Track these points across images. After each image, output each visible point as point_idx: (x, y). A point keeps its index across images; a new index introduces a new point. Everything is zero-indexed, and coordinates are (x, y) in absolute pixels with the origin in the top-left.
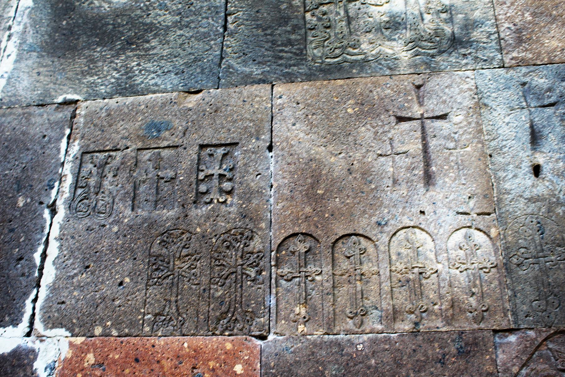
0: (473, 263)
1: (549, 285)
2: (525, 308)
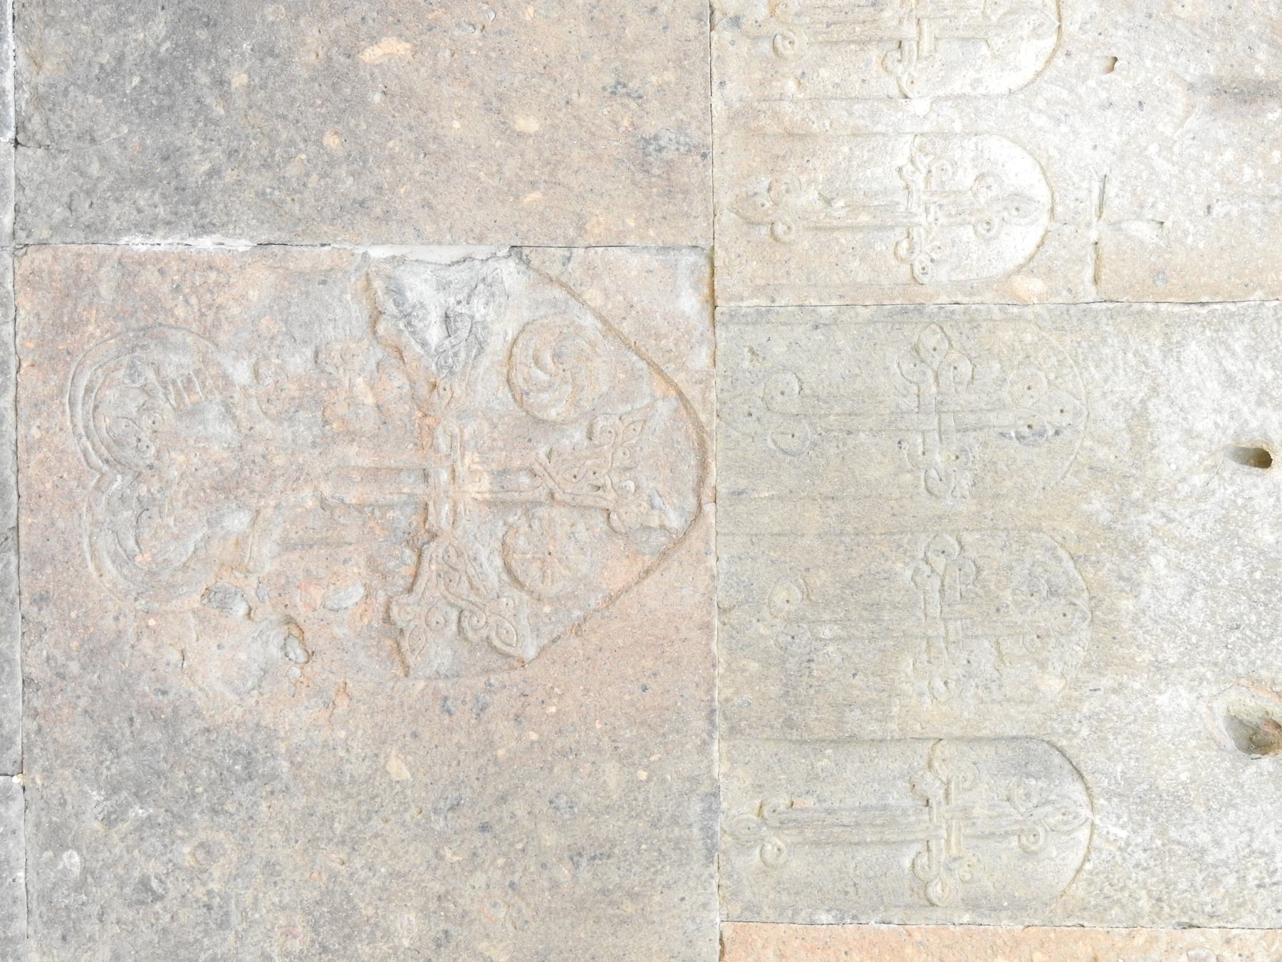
0: (927, 210)
1: (849, 433)
2: (776, 350)
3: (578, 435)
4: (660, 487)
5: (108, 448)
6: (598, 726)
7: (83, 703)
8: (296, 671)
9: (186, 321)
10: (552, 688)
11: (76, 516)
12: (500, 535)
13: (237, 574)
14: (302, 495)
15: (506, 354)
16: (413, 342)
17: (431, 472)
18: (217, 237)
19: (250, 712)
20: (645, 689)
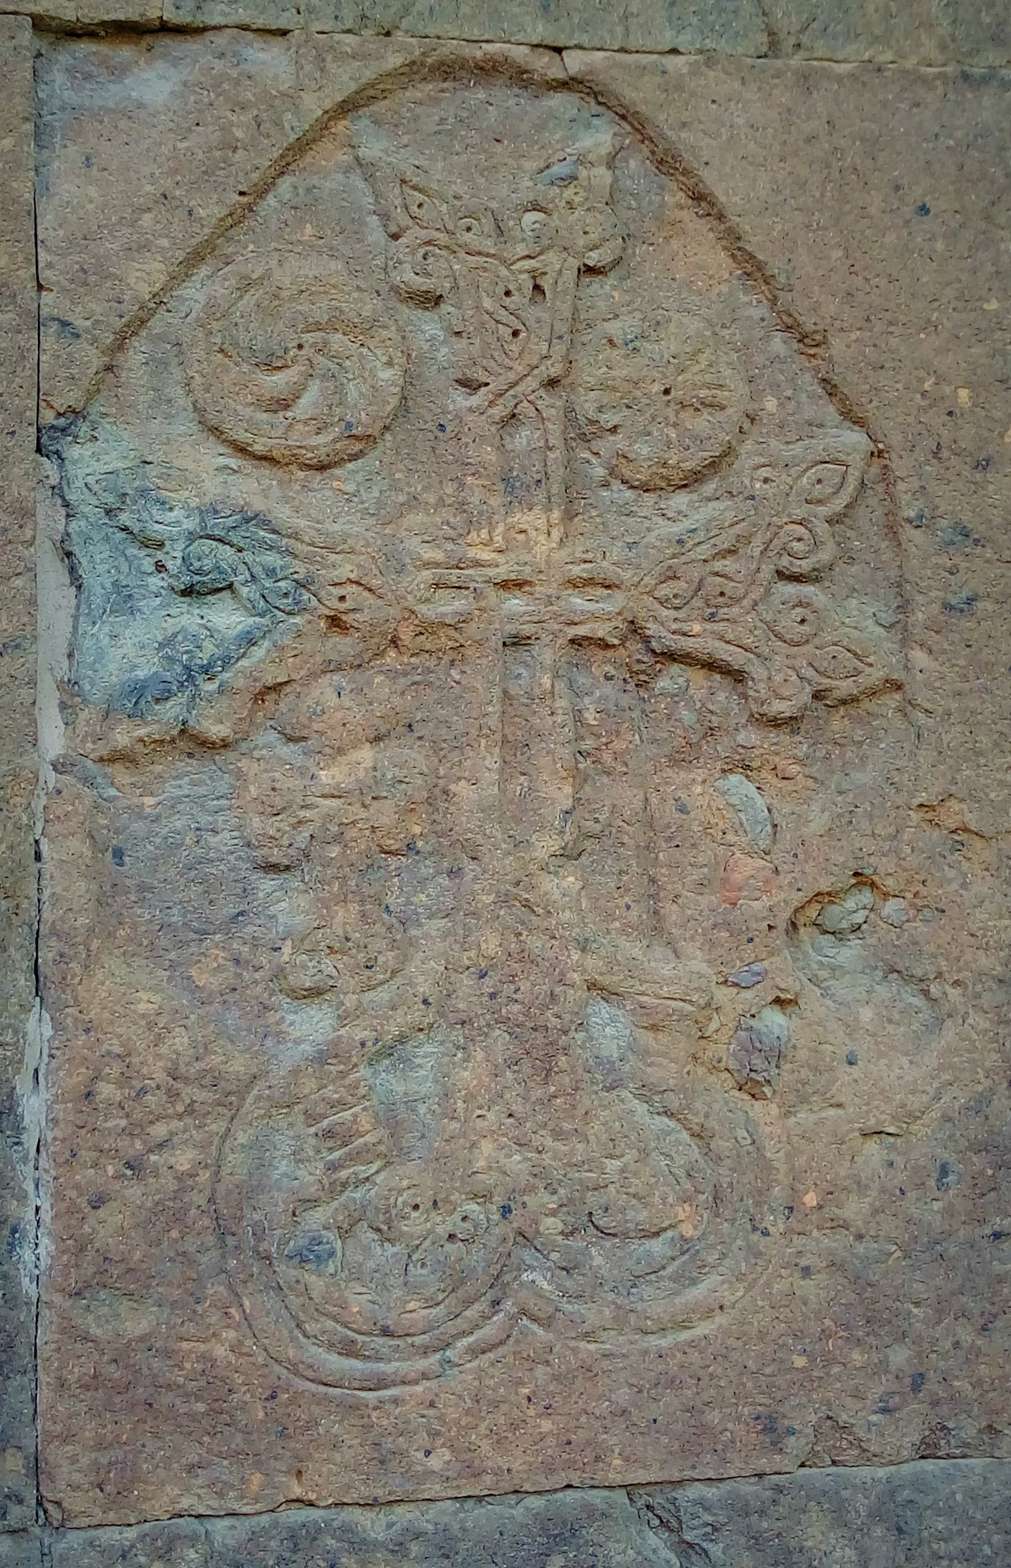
3: (429, 326)
4: (531, 165)
5: (468, 1303)
6: (993, 305)
7: (966, 1335)
8: (891, 908)
9: (203, 1146)
10: (924, 394)
11: (605, 1364)
12: (629, 494)
13: (714, 1026)
14: (556, 895)
15: (266, 471)
16: (244, 663)
17: (511, 628)
18: (22, 1084)
19: (978, 996)
20: (924, 210)
